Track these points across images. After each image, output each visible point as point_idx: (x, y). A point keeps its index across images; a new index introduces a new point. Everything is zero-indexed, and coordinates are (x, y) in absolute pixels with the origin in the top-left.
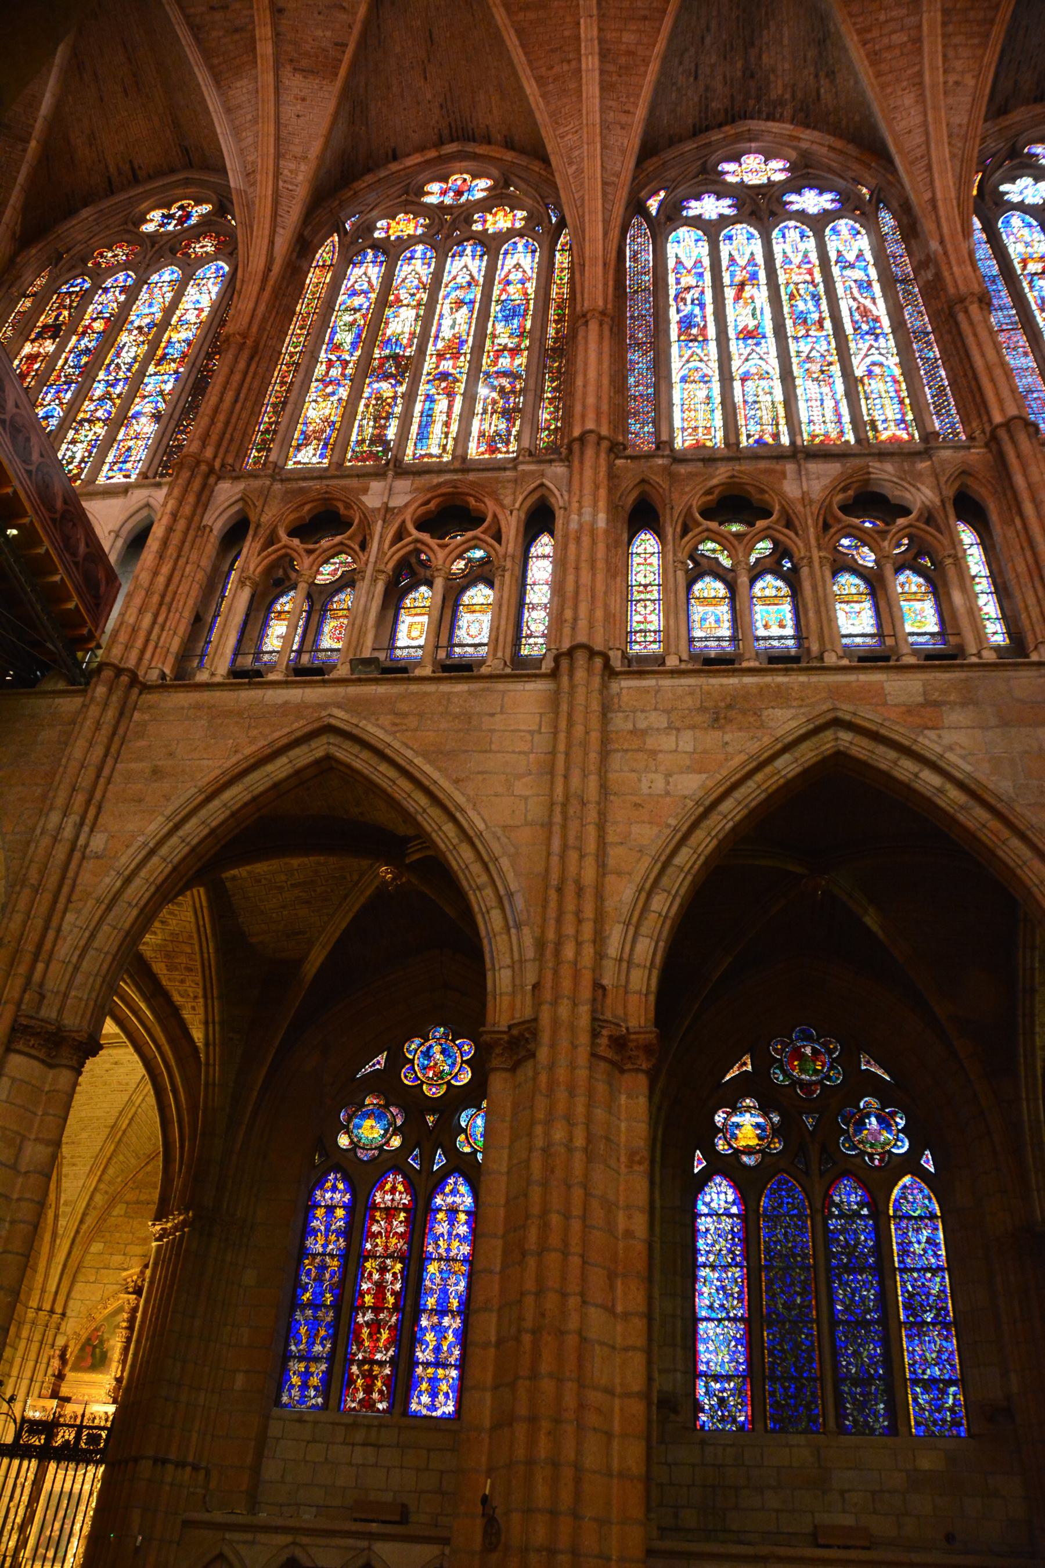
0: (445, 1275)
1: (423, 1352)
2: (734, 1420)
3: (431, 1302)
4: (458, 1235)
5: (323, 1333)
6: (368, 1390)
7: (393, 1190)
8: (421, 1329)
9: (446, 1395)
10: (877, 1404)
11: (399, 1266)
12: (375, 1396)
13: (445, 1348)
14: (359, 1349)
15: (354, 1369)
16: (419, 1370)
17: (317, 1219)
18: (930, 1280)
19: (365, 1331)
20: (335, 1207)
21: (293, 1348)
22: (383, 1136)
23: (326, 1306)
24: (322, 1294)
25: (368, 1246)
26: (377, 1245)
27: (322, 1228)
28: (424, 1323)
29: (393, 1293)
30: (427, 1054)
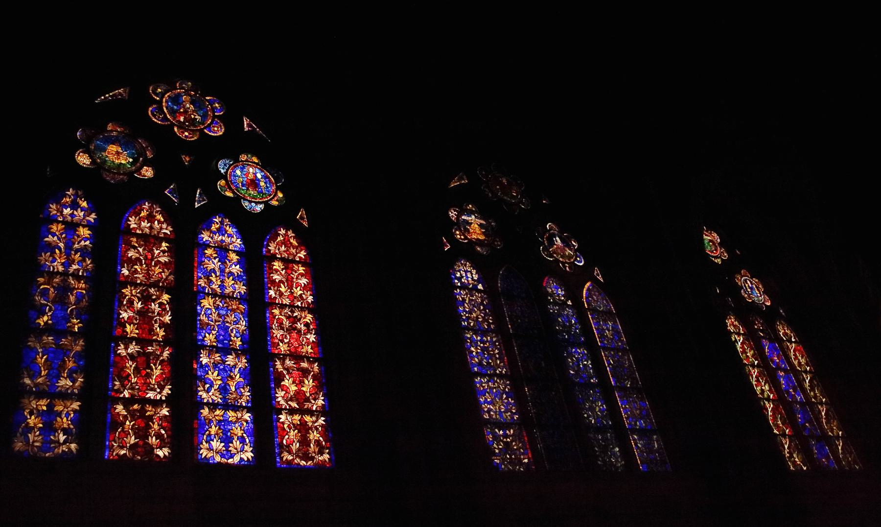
0: (223, 312)
1: (208, 391)
2: (521, 463)
3: (210, 339)
4: (231, 274)
5: (71, 365)
6: (142, 433)
7: (151, 218)
8: (202, 366)
9: (242, 440)
10: (614, 448)
11: (166, 297)
12: (153, 440)
13: (233, 389)
14: (124, 386)
15: (120, 408)
16: (205, 412)
17: (54, 235)
18: (621, 357)
19: (130, 365)
20: (78, 225)
21: (27, 381)
22: (132, 164)
23: (73, 334)
24: (67, 319)
25: (125, 272)
26: (136, 271)
27: (62, 245)
28: (204, 360)
29: (162, 325)
30: (176, 100)
